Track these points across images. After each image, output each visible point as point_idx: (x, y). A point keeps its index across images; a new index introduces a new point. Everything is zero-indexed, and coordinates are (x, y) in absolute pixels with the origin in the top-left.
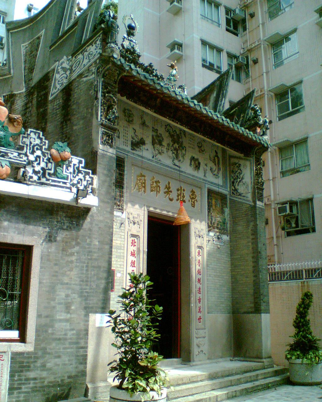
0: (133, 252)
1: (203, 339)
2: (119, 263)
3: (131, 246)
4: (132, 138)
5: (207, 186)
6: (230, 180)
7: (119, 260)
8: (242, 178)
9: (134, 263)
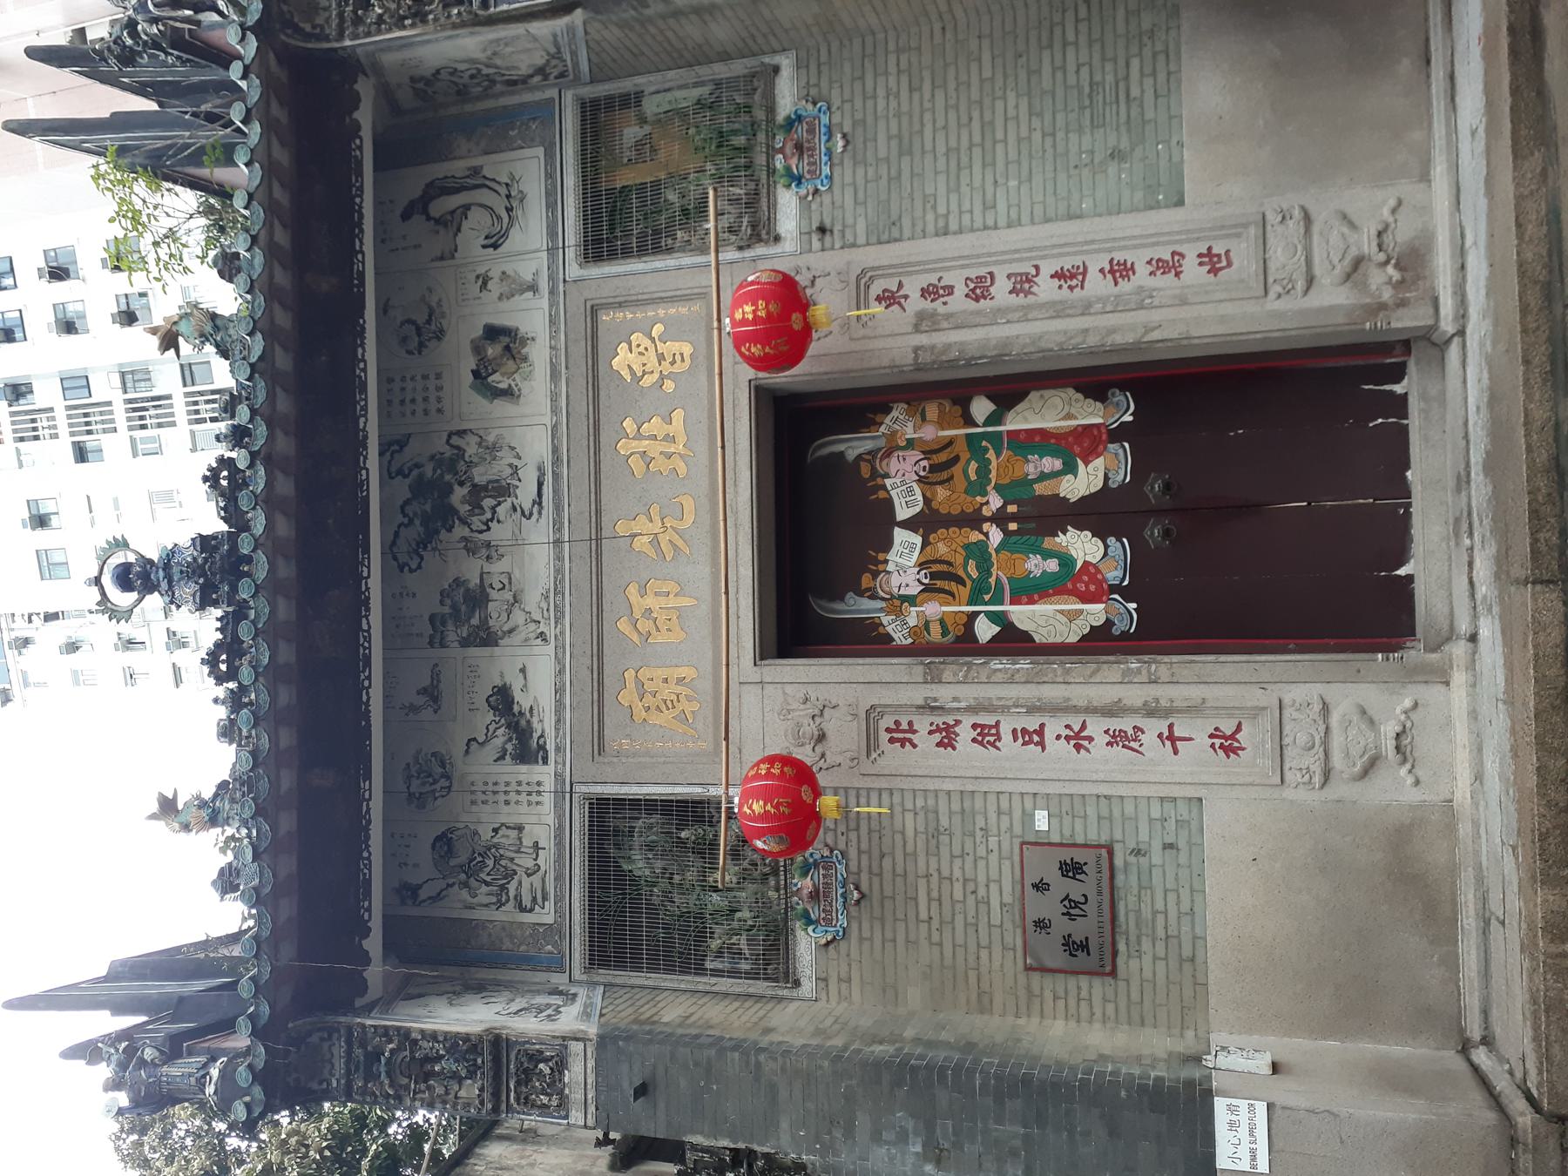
0: (937, 737)
1: (1316, 229)
2: (993, 816)
3: (914, 746)
4: (502, 758)
5: (574, 270)
6: (502, 94)
7: (980, 822)
8: (473, 61)
9: (983, 726)
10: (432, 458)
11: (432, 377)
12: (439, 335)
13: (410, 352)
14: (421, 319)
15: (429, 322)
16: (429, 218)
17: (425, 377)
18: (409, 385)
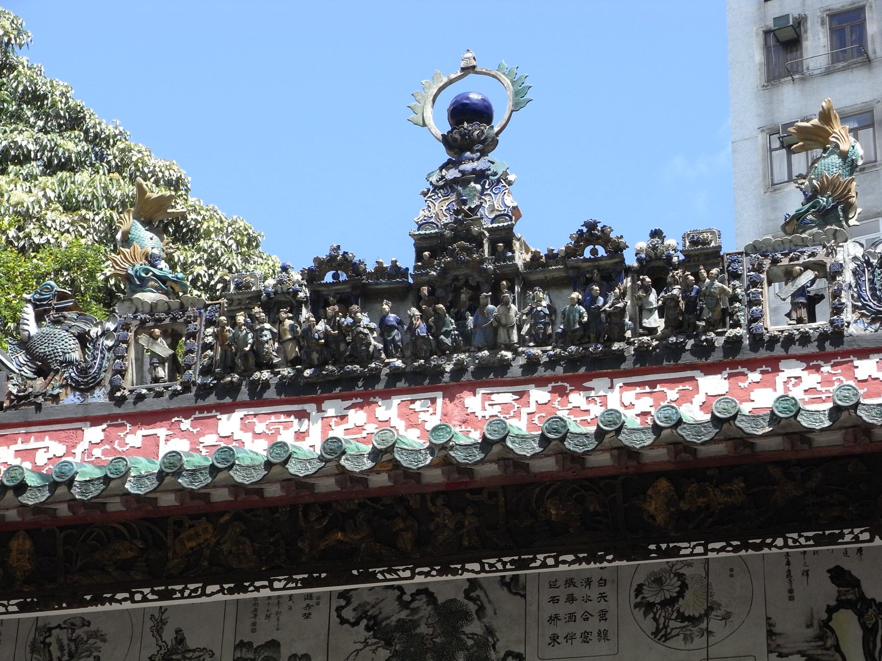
10: (490, 631)
11: (603, 625)
12: (661, 634)
13: (639, 590)
14: (691, 605)
15: (681, 617)
16: (831, 610)
17: (603, 615)
18: (594, 592)
